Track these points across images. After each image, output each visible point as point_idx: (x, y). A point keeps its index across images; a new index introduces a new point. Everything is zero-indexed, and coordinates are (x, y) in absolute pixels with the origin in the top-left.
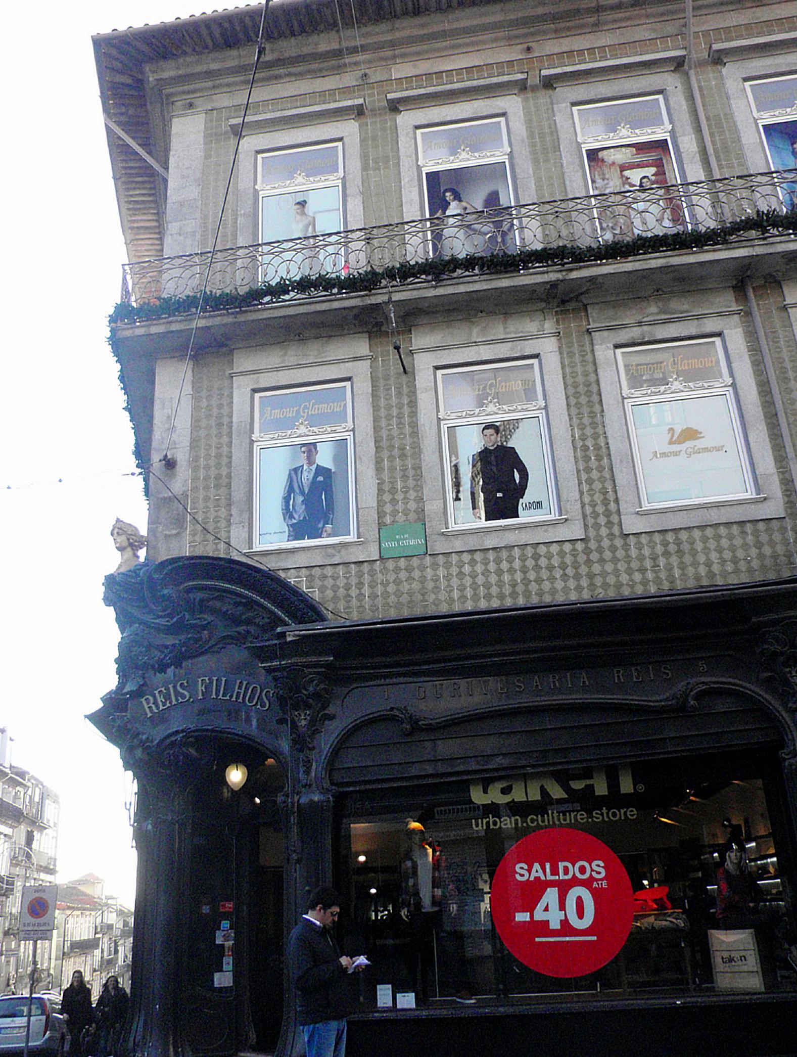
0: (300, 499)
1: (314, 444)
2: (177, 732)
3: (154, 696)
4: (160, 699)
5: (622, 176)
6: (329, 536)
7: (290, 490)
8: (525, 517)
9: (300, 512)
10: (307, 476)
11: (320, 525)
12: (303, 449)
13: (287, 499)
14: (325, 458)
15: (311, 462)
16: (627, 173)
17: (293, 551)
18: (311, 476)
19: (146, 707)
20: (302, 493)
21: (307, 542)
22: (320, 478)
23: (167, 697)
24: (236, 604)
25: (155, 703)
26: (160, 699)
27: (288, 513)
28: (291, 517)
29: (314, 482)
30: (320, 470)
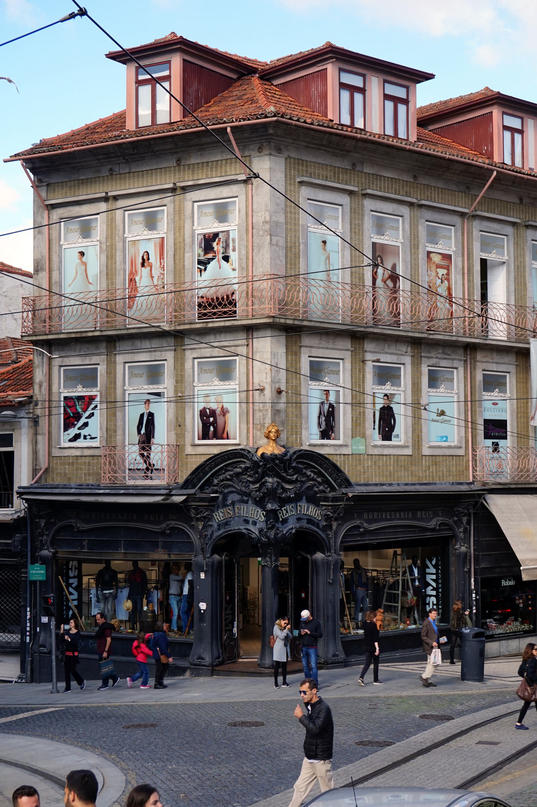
0: (324, 418)
1: (328, 391)
2: (292, 528)
3: (282, 511)
4: (285, 512)
5: (436, 271)
6: (333, 439)
7: (320, 413)
8: (394, 442)
9: (323, 426)
10: (326, 407)
11: (330, 433)
12: (325, 392)
13: (319, 417)
14: (332, 398)
15: (327, 400)
16: (438, 270)
17: (323, 445)
18: (327, 408)
19: (280, 516)
20: (324, 416)
21: (325, 441)
22: (330, 409)
23: (287, 512)
24: (311, 471)
25: (283, 514)
26: (285, 512)
27: (319, 425)
28: (321, 427)
29: (328, 411)
30: (331, 406)
